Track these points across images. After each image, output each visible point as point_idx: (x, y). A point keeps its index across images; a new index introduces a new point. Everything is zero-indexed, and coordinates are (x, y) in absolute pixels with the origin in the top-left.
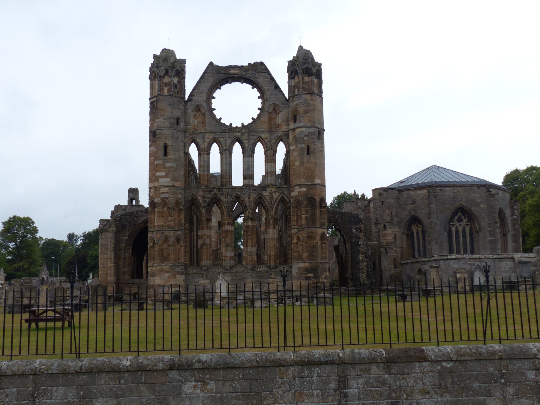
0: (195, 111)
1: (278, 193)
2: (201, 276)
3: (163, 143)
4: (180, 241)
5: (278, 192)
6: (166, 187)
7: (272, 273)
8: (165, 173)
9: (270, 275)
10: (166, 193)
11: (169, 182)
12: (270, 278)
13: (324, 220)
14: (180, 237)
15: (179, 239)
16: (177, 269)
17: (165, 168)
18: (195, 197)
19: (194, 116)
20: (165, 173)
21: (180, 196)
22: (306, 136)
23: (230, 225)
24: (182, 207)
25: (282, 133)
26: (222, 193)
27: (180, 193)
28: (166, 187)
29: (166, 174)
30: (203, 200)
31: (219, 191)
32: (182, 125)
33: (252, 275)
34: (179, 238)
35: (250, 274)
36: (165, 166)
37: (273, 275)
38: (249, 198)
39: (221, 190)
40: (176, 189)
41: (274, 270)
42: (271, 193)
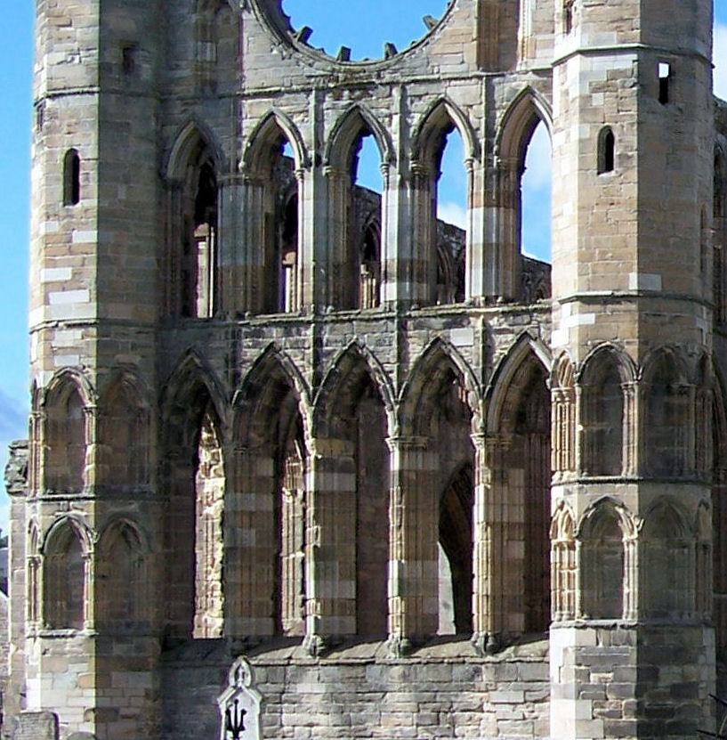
0: (205, 7)
1: (510, 337)
2: (217, 676)
3: (67, 149)
4: (132, 539)
5: (512, 332)
6: (74, 326)
7: (483, 667)
8: (70, 269)
9: (472, 678)
10: (75, 349)
11: (80, 305)
12: (472, 689)
13: (681, 444)
14: (133, 524)
15: (130, 533)
16: (118, 649)
17: (71, 252)
18: (197, 361)
19: (204, 27)
20: (70, 269)
21: (137, 360)
22: (597, 89)
23: (332, 470)
24: (144, 404)
25: (536, 78)
26: (297, 341)
27: (134, 347)
28: (74, 326)
29: (74, 274)
30: (227, 372)
31: (288, 334)
32: (146, 71)
33: (405, 677)
34: (128, 526)
35: (397, 670)
36: (70, 241)
37: (487, 676)
38: (402, 357)
39: (294, 330)
40: (113, 329)
41: (489, 658)
42: (487, 332)
